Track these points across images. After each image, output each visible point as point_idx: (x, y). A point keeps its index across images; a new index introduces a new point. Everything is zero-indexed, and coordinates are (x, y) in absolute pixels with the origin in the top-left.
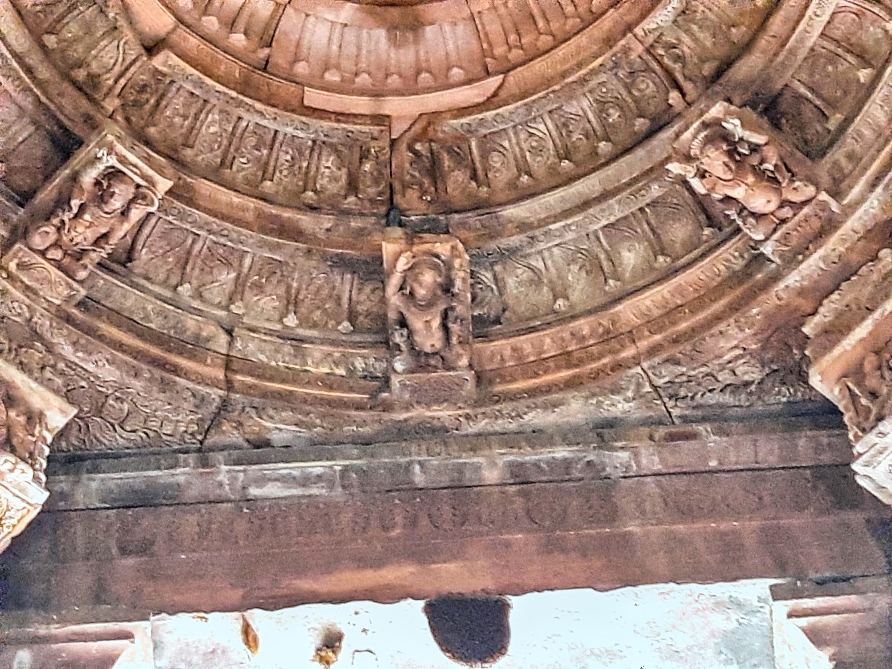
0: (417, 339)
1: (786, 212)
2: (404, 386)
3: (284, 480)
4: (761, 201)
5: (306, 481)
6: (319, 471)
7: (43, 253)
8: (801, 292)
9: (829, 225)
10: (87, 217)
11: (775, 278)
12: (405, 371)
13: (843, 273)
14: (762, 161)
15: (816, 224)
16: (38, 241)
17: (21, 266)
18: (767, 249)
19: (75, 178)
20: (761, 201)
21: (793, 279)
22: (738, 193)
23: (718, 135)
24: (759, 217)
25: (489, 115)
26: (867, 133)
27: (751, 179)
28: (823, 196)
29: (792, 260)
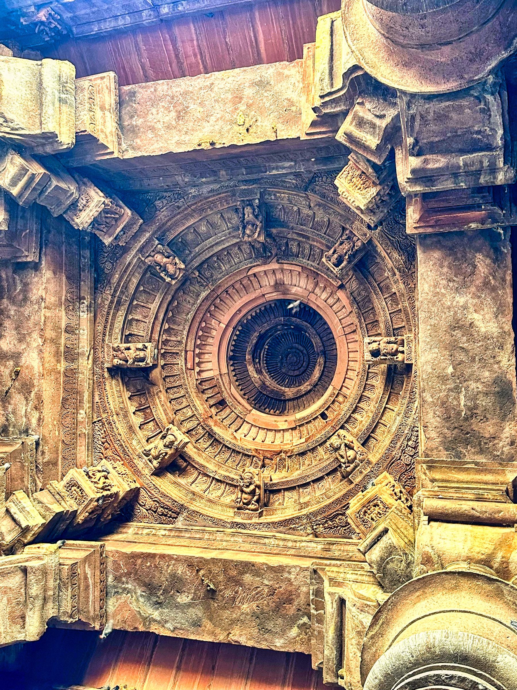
0: (251, 211)
1: (152, 254)
2: (256, 194)
3: (284, 168)
4: (159, 258)
5: (277, 168)
6: (274, 171)
7: (359, 239)
8: (145, 231)
9: (141, 250)
10: (345, 251)
11: (153, 234)
12: (255, 199)
13: (135, 237)
14: (160, 269)
15: (145, 250)
16: (359, 244)
17: (365, 235)
18: (157, 242)
19: (349, 262)
20: (159, 258)
21: (148, 235)
22: (165, 260)
23: (172, 277)
24: (159, 252)
25: (249, 265)
26: (137, 274)
27: (162, 264)
28: (143, 259)
29: (149, 241)
